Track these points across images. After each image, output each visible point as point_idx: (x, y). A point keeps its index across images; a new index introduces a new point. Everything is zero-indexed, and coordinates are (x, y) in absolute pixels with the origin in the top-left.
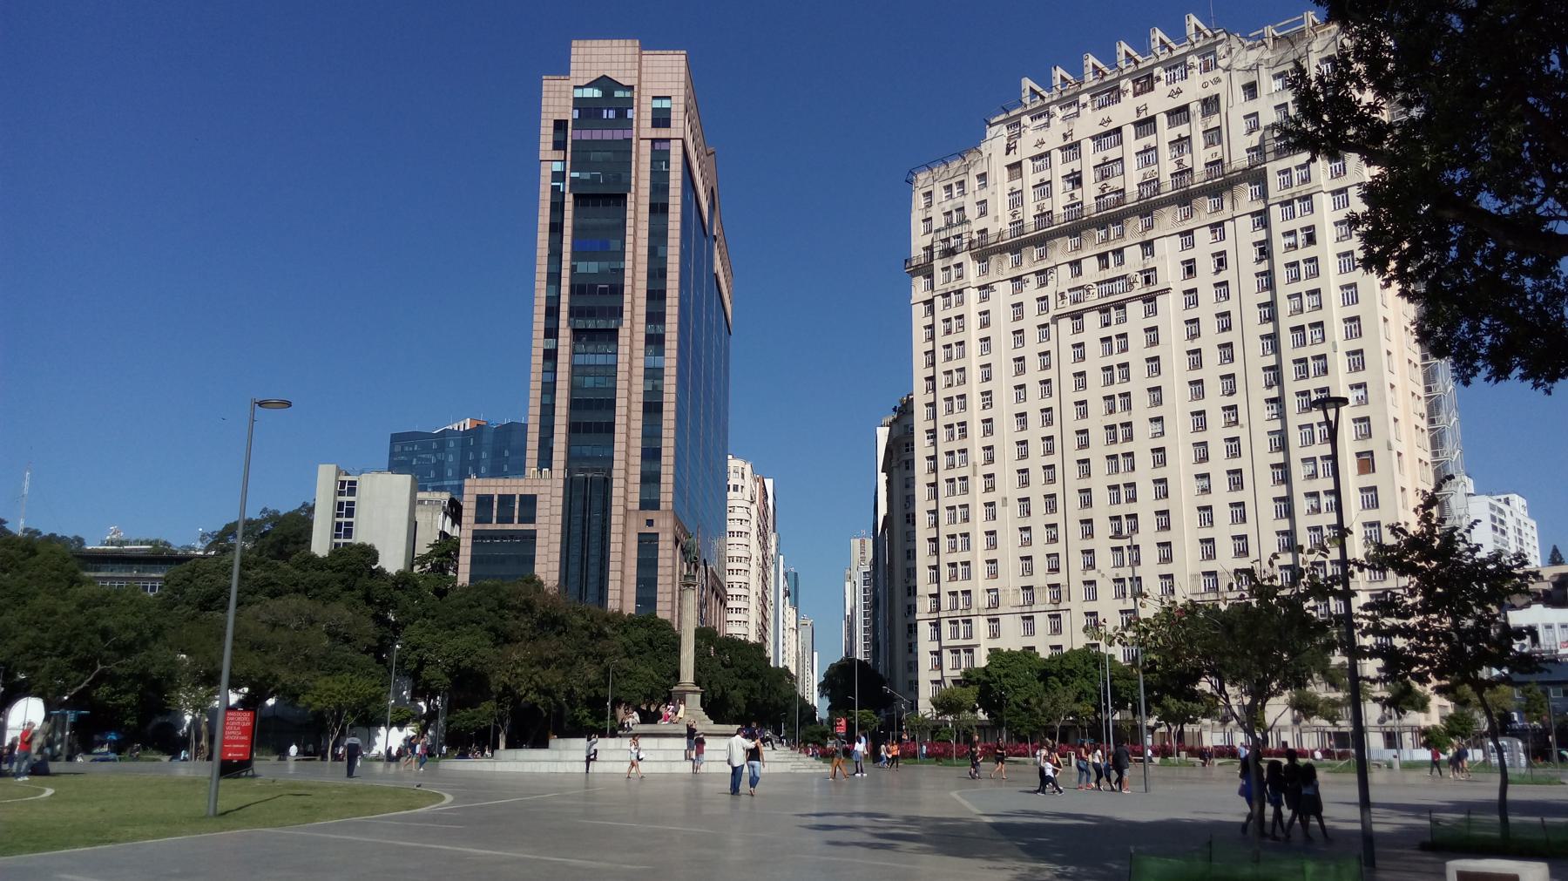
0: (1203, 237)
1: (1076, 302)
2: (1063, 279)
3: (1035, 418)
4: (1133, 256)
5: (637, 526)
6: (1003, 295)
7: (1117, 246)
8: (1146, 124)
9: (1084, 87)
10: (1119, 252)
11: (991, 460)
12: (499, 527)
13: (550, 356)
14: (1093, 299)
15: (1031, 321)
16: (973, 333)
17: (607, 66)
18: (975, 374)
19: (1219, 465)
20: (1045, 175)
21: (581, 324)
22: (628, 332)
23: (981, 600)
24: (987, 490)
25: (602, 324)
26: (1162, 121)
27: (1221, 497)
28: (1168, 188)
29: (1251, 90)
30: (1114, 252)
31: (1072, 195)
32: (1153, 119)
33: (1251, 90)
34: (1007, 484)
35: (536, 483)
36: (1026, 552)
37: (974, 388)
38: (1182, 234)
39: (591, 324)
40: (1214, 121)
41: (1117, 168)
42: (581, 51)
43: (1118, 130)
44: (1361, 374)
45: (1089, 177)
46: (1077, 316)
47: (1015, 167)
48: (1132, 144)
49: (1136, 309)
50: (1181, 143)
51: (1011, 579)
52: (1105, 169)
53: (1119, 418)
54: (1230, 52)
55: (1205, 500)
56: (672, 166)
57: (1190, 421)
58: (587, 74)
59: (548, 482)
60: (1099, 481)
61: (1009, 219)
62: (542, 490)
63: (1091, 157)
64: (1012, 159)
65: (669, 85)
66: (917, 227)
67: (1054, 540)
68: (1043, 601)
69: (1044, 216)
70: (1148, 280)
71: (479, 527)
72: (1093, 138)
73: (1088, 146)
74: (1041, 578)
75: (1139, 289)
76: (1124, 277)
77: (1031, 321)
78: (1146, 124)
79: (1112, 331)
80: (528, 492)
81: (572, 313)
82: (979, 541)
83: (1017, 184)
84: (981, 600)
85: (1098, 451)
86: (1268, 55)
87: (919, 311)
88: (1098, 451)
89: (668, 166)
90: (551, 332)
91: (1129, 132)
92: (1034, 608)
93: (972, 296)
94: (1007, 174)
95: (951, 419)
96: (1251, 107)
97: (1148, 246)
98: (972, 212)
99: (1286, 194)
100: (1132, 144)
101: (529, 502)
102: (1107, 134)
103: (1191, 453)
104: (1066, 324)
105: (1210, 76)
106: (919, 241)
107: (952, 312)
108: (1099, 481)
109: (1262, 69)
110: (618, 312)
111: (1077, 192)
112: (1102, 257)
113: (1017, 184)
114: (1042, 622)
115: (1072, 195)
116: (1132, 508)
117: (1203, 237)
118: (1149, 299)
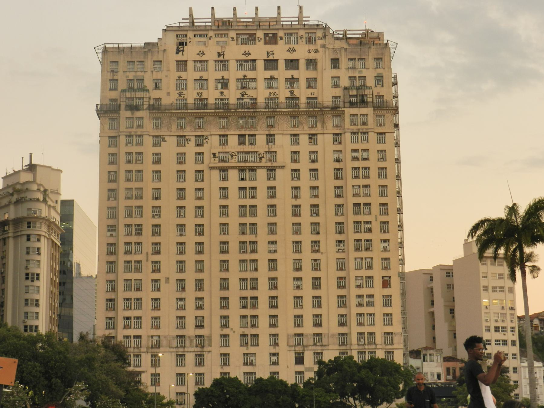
0: (304, 139)
1: (223, 161)
2: (213, 144)
3: (190, 230)
4: (261, 140)
7: (252, 133)
8: (271, 64)
11: (158, 252)
14: (233, 162)
15: (190, 167)
16: (148, 167)
19: (307, 274)
23: (145, 342)
24: (153, 271)
26: (281, 64)
27: (308, 292)
29: (335, 63)
30: (249, 135)
31: (222, 93)
33: (335, 63)
38: (291, 135)
41: (252, 84)
43: (254, 61)
44: (387, 235)
45: (233, 84)
46: (223, 170)
47: (182, 65)
49: (262, 174)
50: (292, 80)
51: (168, 329)
53: (248, 238)
55: (298, 293)
57: (290, 245)
60: (234, 276)
64: (180, 57)
72: (237, 61)
73: (233, 65)
74: (191, 331)
76: (257, 152)
77: (190, 167)
78: (271, 64)
79: (247, 184)
82: (147, 304)
83: (183, 75)
85: (234, 256)
91: (260, 65)
92: (186, 349)
93: (148, 141)
95: (129, 221)
96: (335, 72)
97: (270, 137)
102: (246, 61)
104: (216, 174)
105: (312, 47)
111: (225, 92)
112: (241, 137)
115: (222, 93)
116: (254, 293)
117: (304, 139)
118: (271, 169)
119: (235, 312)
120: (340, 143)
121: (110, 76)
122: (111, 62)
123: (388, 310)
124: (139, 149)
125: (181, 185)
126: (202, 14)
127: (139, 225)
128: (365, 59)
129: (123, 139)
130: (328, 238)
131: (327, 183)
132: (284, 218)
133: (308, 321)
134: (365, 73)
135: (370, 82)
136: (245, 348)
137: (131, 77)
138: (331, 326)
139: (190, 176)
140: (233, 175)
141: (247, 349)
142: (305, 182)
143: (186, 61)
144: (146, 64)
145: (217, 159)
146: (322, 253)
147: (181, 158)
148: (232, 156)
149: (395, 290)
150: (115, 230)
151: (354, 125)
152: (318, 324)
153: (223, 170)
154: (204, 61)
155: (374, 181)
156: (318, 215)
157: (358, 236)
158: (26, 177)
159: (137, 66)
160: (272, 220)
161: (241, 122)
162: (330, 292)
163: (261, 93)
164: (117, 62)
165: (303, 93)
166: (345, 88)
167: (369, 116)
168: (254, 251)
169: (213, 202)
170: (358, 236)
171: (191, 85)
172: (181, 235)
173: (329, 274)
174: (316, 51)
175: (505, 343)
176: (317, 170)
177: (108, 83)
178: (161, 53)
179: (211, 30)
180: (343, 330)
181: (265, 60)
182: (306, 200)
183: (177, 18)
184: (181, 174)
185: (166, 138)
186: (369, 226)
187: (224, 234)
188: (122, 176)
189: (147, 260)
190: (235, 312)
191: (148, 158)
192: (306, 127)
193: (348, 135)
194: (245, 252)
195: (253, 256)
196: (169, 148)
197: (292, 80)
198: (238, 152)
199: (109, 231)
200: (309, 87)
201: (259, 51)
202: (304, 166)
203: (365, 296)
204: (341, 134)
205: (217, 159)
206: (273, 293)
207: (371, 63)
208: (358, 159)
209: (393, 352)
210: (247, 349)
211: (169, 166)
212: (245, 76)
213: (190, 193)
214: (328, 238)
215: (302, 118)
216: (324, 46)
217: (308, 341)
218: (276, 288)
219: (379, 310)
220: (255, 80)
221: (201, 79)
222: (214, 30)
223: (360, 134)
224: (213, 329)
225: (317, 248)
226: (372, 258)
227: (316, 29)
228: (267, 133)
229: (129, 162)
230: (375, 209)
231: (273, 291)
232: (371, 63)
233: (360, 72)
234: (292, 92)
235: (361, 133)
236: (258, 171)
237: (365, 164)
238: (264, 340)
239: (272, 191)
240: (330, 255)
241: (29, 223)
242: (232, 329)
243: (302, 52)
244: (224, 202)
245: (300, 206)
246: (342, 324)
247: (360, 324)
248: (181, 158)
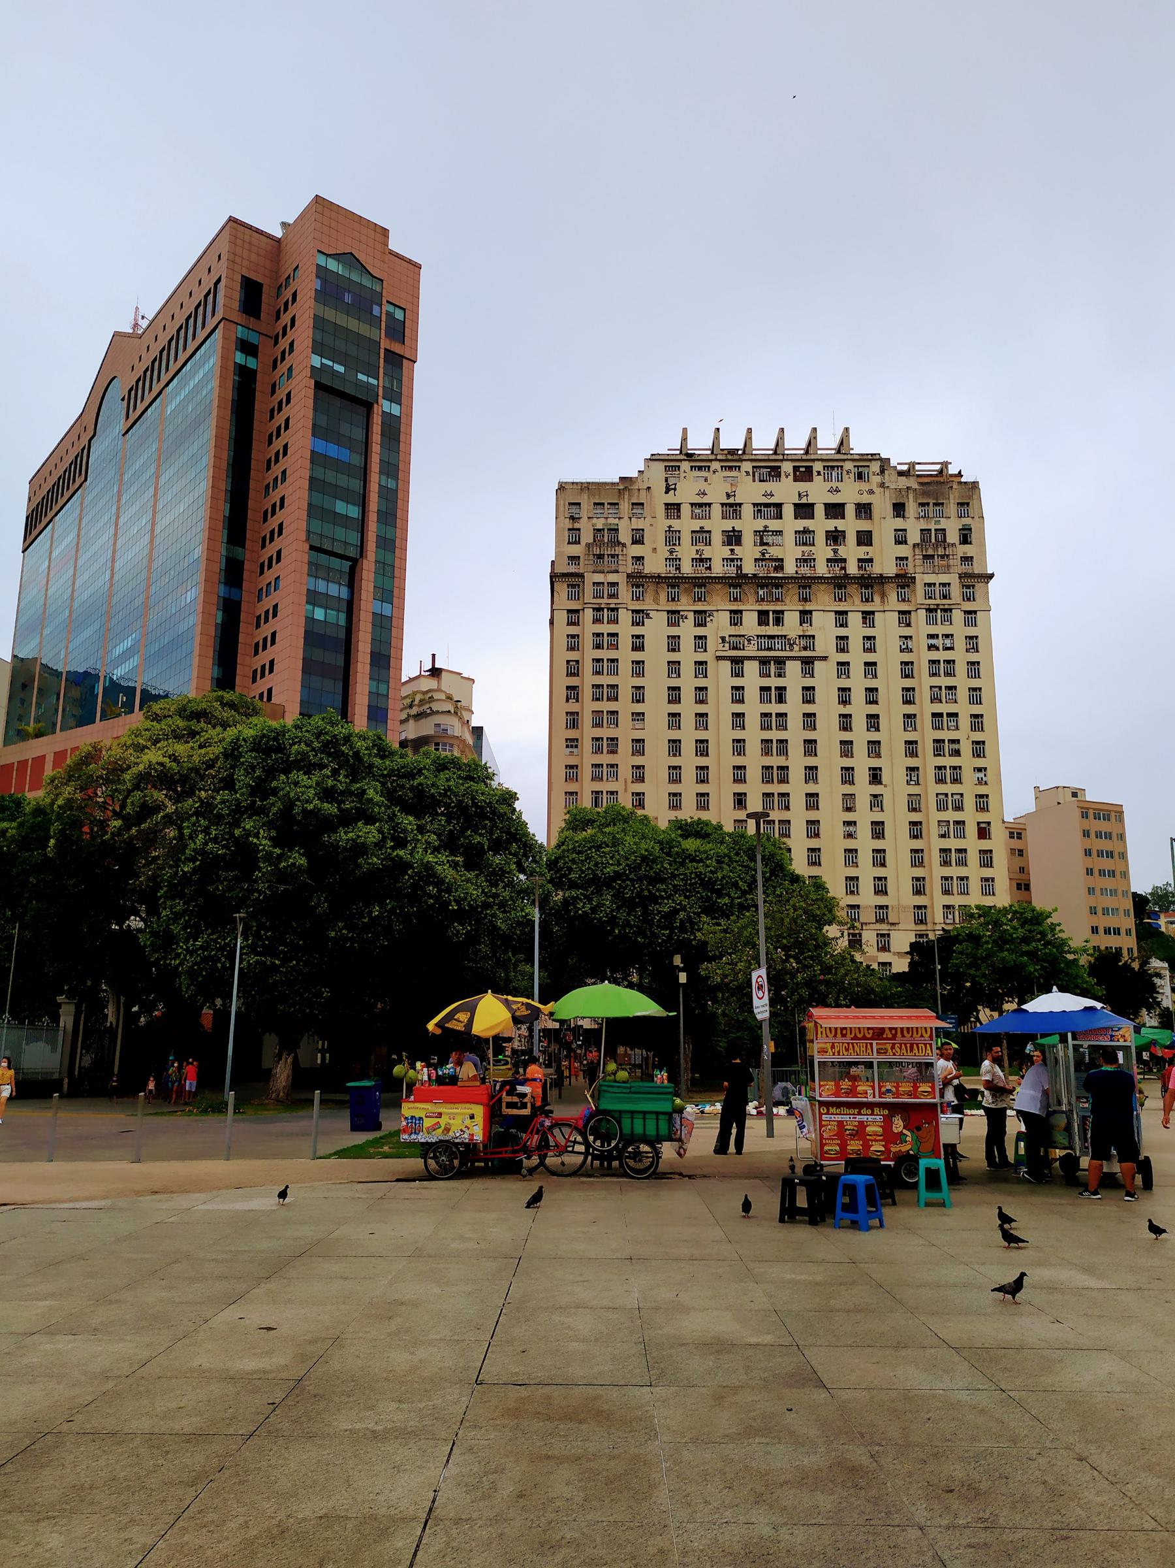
0: (855, 619)
1: (735, 648)
2: (720, 625)
3: (688, 747)
4: (791, 620)
7: (778, 608)
11: (641, 779)
15: (687, 656)
16: (625, 655)
19: (864, 816)
26: (819, 511)
27: (865, 843)
30: (774, 612)
31: (732, 550)
32: (811, 506)
33: (899, 509)
38: (837, 612)
43: (779, 506)
45: (748, 538)
47: (673, 509)
48: (790, 524)
49: (793, 668)
50: (835, 537)
53: (775, 761)
55: (850, 843)
63: (748, 524)
64: (671, 498)
72: (754, 505)
73: (747, 511)
77: (687, 656)
78: (804, 510)
79: (773, 682)
83: (676, 524)
91: (788, 511)
93: (625, 616)
95: (598, 733)
96: (899, 523)
102: (767, 505)
105: (865, 486)
109: (911, 496)
115: (732, 550)
117: (855, 619)
118: (808, 662)
120: (909, 625)
121: (568, 524)
122: (570, 504)
123: (987, 873)
124: (612, 628)
125: (674, 683)
126: (700, 442)
127: (612, 739)
128: (942, 504)
130: (894, 764)
131: (890, 683)
132: (828, 734)
138: (901, 895)
139: (688, 669)
140: (751, 668)
143: (679, 505)
144: (621, 507)
147: (674, 644)
148: (749, 641)
149: (998, 843)
150: (576, 746)
151: (930, 598)
152: (881, 891)
153: (737, 661)
154: (706, 504)
155: (962, 681)
156: (878, 730)
157: (941, 761)
158: (430, 684)
159: (608, 510)
160: (811, 735)
161: (761, 592)
162: (898, 843)
163: (789, 553)
164: (579, 504)
165: (851, 552)
168: (784, 780)
169: (721, 707)
170: (941, 761)
173: (897, 818)
174: (871, 492)
175: (1117, 932)
176: (875, 664)
177: (566, 533)
178: (643, 493)
179: (716, 460)
180: (921, 900)
181: (795, 505)
183: (668, 444)
184: (674, 667)
185: (652, 614)
186: (956, 746)
187: (739, 754)
188: (588, 667)
189: (626, 790)
191: (625, 642)
192: (857, 600)
193: (922, 613)
195: (783, 788)
196: (656, 629)
197: (835, 537)
199: (567, 746)
201: (786, 491)
202: (856, 657)
204: (909, 612)
205: (727, 645)
206: (814, 843)
207: (952, 509)
208: (937, 649)
211: (656, 655)
212: (766, 527)
213: (688, 695)
214: (894, 764)
215: (853, 589)
216: (882, 485)
217: (867, 916)
218: (817, 835)
219: (974, 871)
221: (702, 530)
222: (720, 460)
226: (962, 795)
227: (870, 460)
229: (598, 646)
230: (965, 721)
232: (952, 509)
233: (937, 522)
234: (835, 551)
237: (948, 655)
239: (809, 694)
240: (896, 788)
241: (437, 744)
243: (850, 493)
244: (738, 708)
245: (850, 716)
246: (918, 891)
248: (674, 644)
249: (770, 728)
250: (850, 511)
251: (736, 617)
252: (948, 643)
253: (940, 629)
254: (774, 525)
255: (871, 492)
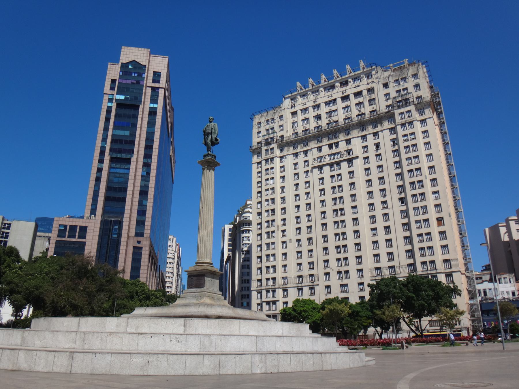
0: (370, 138)
1: (320, 162)
2: (314, 153)
5: (133, 243)
6: (290, 161)
7: (336, 141)
8: (345, 98)
9: (321, 85)
10: (338, 143)
11: (285, 225)
12: (69, 239)
13: (100, 170)
14: (327, 160)
15: (301, 169)
16: (278, 174)
17: (136, 57)
18: (278, 190)
19: (380, 224)
20: (307, 116)
21: (114, 155)
22: (135, 160)
23: (280, 282)
24: (283, 236)
25: (124, 156)
27: (382, 237)
28: (355, 119)
29: (386, 85)
30: (335, 143)
31: (317, 123)
33: (386, 85)
34: (291, 234)
35: (88, 221)
36: (299, 261)
37: (278, 195)
39: (119, 156)
40: (373, 96)
41: (335, 113)
42: (126, 50)
45: (324, 116)
47: (294, 114)
48: (340, 105)
49: (344, 165)
50: (359, 104)
51: (293, 272)
52: (330, 113)
54: (377, 72)
55: (375, 239)
56: (159, 98)
58: (127, 59)
59: (94, 221)
60: (331, 231)
61: (292, 132)
62: (90, 224)
63: (324, 110)
64: (293, 110)
65: (160, 68)
66: (255, 135)
67: (311, 256)
68: (307, 281)
69: (306, 131)
70: (349, 154)
71: (59, 239)
72: (325, 103)
73: (323, 106)
74: (306, 272)
75: (346, 156)
77: (301, 169)
79: (335, 173)
80: (84, 225)
81: (112, 150)
83: (295, 119)
84: (280, 282)
85: (330, 219)
86: (392, 73)
87: (255, 167)
88: (330, 219)
89: (158, 98)
90: (101, 161)
91: (339, 101)
93: (277, 160)
94: (291, 117)
96: (386, 91)
97: (348, 142)
98: (277, 129)
99: (403, 121)
100: (340, 105)
101: (84, 230)
102: (331, 101)
103: (369, 221)
104: (316, 171)
106: (256, 140)
107: (269, 166)
108: (331, 231)
110: (132, 152)
111: (320, 122)
113: (295, 119)
114: (306, 290)
115: (317, 123)
117: (370, 138)
118: (350, 161)
119: (333, 255)
129: (263, 163)
133: (384, 258)
134: (406, 85)
135: (411, 89)
136: (341, 281)
137: (268, 128)
138: (402, 260)
140: (327, 169)
141: (342, 281)
142: (373, 163)
145: (316, 162)
146: (389, 209)
152: (391, 259)
153: (320, 168)
166: (394, 98)
167: (412, 112)
171: (300, 123)
172: (298, 212)
174: (373, 82)
178: (283, 111)
182: (375, 175)
189: (278, 230)
190: (333, 255)
194: (337, 216)
198: (329, 155)
200: (371, 104)
203: (424, 235)
205: (316, 162)
209: (452, 275)
210: (342, 281)
220: (336, 110)
223: (407, 124)
224: (320, 269)
225: (386, 206)
228: (345, 138)
231: (357, 239)
235: (408, 123)
236: (342, 164)
238: (353, 274)
242: (331, 268)
247: (423, 255)
249: (336, 193)
250: (365, 93)
251: (320, 149)
252: (413, 137)
253: (408, 132)
254: (333, 108)
255: (373, 82)
